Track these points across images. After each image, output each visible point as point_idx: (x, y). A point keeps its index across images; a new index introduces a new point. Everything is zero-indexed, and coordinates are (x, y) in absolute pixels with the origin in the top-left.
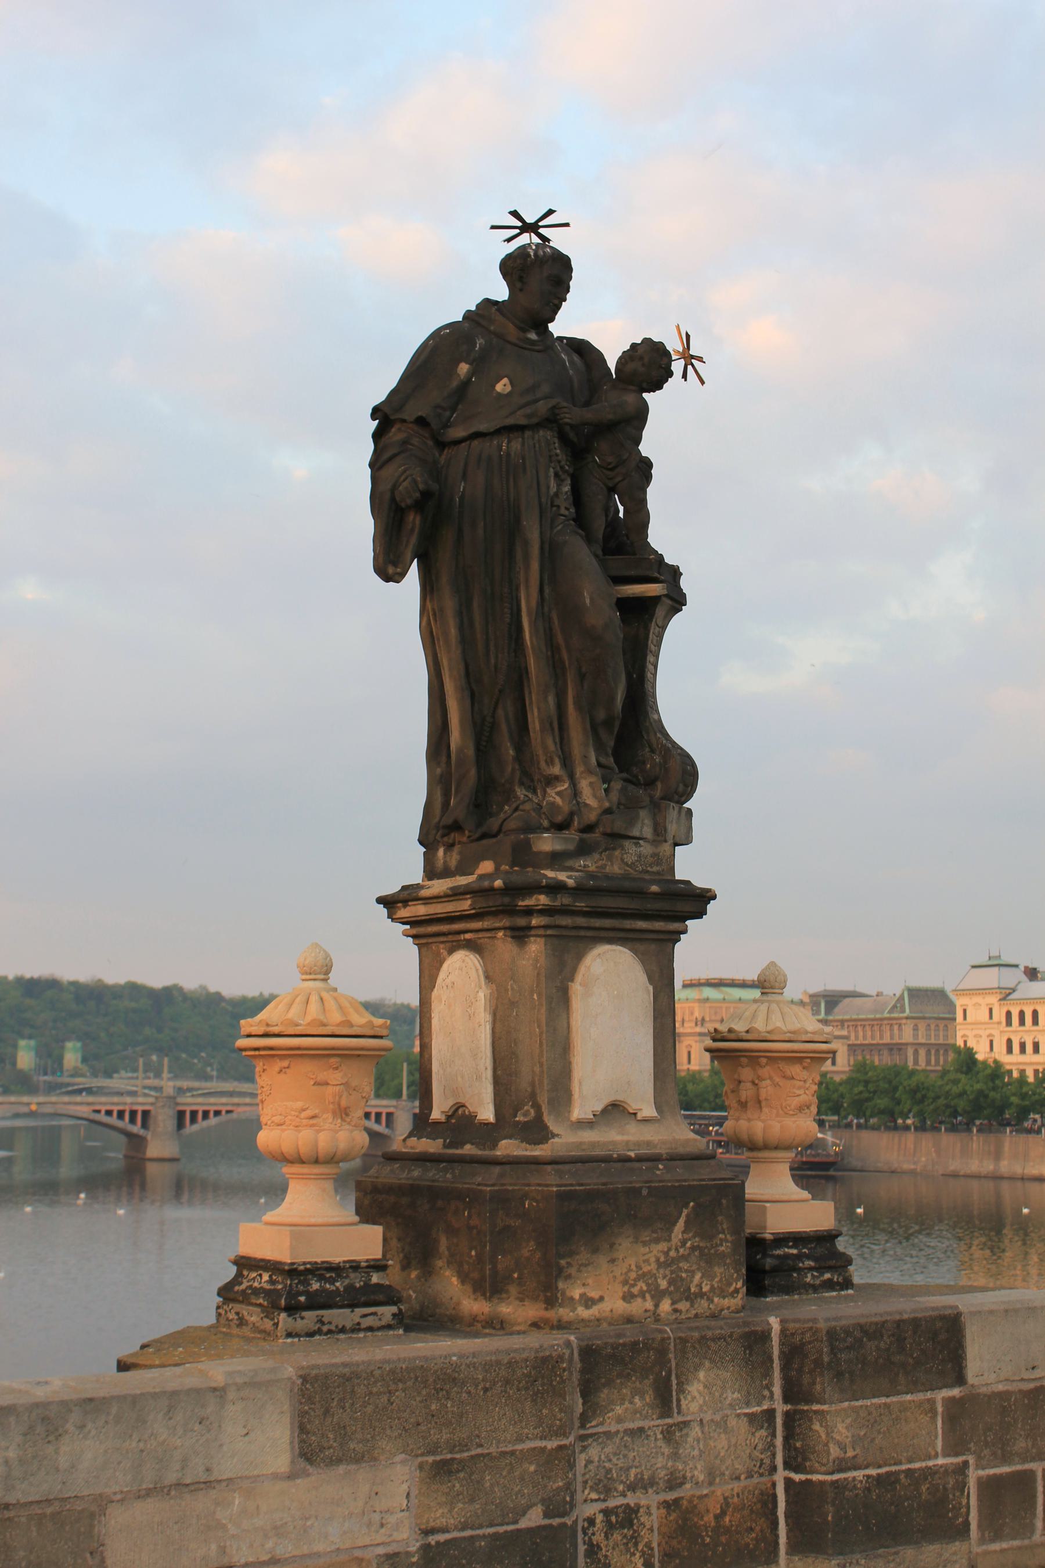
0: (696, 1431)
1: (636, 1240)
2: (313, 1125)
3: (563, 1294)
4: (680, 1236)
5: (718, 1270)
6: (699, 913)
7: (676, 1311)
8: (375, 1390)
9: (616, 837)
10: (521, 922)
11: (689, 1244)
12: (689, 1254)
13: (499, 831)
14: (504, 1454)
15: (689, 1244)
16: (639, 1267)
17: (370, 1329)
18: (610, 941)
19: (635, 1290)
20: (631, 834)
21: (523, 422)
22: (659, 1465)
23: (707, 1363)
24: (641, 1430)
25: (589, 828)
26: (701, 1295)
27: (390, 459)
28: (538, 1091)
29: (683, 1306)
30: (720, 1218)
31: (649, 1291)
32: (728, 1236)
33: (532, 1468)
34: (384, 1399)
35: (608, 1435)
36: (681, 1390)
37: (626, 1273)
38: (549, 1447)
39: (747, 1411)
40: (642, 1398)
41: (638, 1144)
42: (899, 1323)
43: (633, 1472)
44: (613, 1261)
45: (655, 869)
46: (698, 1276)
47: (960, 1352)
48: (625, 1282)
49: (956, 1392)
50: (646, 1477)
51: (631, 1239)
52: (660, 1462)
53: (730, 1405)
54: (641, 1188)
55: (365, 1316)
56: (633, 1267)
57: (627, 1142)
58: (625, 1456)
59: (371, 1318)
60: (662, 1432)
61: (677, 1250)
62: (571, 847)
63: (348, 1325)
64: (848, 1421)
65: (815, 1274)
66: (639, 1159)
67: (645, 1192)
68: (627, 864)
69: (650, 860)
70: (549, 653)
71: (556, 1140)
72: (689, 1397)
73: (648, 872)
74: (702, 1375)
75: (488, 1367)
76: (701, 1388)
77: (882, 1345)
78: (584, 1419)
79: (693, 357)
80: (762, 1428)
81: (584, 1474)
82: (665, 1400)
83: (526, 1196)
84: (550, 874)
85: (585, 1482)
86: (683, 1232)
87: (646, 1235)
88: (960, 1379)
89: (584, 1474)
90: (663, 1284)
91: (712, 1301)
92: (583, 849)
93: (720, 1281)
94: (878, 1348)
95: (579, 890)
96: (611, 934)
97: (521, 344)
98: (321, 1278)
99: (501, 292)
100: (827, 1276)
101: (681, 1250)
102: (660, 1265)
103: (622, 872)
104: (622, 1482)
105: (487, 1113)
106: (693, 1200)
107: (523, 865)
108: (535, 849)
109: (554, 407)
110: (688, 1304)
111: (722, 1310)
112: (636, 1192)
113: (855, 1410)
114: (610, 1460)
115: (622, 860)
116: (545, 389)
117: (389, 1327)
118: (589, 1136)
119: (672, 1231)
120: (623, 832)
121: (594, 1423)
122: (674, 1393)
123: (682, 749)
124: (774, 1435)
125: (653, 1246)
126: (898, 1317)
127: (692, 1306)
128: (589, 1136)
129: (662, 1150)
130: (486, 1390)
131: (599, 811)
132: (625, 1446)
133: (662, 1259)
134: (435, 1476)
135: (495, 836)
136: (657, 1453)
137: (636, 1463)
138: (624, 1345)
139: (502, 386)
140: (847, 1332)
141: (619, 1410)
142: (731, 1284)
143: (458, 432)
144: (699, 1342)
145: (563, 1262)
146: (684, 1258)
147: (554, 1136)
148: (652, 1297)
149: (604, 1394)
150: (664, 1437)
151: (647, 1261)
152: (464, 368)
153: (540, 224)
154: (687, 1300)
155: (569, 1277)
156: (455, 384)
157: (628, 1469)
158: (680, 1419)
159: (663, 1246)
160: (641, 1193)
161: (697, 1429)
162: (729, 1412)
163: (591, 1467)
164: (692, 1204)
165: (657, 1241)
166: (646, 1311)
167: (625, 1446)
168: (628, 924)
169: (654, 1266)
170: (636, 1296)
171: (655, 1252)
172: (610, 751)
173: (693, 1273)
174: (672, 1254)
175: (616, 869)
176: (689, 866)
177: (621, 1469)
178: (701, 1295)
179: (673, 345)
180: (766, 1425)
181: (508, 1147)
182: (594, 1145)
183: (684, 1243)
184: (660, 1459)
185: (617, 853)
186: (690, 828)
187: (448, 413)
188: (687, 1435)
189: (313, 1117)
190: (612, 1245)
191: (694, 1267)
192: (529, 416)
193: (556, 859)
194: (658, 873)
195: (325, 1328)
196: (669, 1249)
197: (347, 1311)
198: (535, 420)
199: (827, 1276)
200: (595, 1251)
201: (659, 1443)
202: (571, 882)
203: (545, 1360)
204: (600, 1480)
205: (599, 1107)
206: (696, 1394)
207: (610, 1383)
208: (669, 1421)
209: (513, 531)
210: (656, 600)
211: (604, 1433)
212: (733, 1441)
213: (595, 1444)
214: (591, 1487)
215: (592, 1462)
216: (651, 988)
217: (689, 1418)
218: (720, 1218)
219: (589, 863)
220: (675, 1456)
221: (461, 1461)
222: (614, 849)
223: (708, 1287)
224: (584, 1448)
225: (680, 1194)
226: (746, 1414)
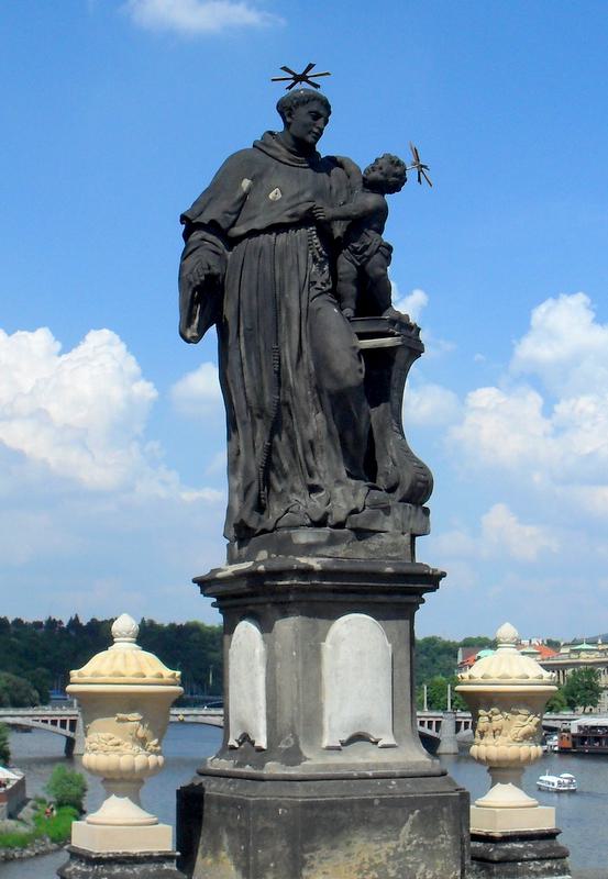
1: (369, 839)
2: (117, 751)
5: (440, 862)
6: (435, 587)
9: (362, 534)
10: (282, 598)
12: (415, 850)
13: (275, 529)
16: (371, 860)
20: (372, 528)
21: (287, 220)
25: (340, 525)
27: (191, 253)
28: (296, 726)
30: (441, 822)
41: (377, 766)
44: (349, 855)
45: (394, 555)
46: (422, 867)
56: (367, 860)
57: (367, 764)
61: (404, 847)
62: (323, 539)
66: (375, 777)
67: (376, 802)
69: (391, 548)
70: (316, 395)
71: (307, 763)
79: (422, 166)
83: (280, 805)
84: (303, 560)
87: (377, 836)
92: (332, 541)
95: (325, 574)
97: (289, 162)
99: (278, 125)
102: (389, 858)
105: (262, 742)
107: (287, 554)
108: (295, 541)
109: (311, 209)
116: (308, 195)
123: (418, 461)
125: (383, 844)
129: (397, 772)
131: (347, 512)
135: (272, 531)
139: (274, 195)
143: (239, 230)
145: (307, 856)
146: (406, 853)
147: (306, 759)
151: (379, 856)
152: (246, 183)
153: (308, 75)
155: (312, 867)
156: (239, 195)
159: (393, 844)
164: (417, 811)
168: (369, 598)
169: (384, 859)
172: (361, 465)
173: (418, 864)
175: (362, 555)
176: (428, 553)
179: (407, 159)
181: (273, 768)
182: (338, 767)
183: (410, 842)
186: (428, 522)
187: (234, 217)
189: (118, 745)
190: (348, 844)
192: (292, 216)
193: (309, 549)
196: (398, 846)
198: (295, 219)
199: (548, 864)
200: (334, 847)
202: (317, 566)
205: (345, 738)
209: (277, 303)
210: (393, 349)
216: (390, 646)
218: (441, 822)
219: (341, 550)
225: (409, 803)
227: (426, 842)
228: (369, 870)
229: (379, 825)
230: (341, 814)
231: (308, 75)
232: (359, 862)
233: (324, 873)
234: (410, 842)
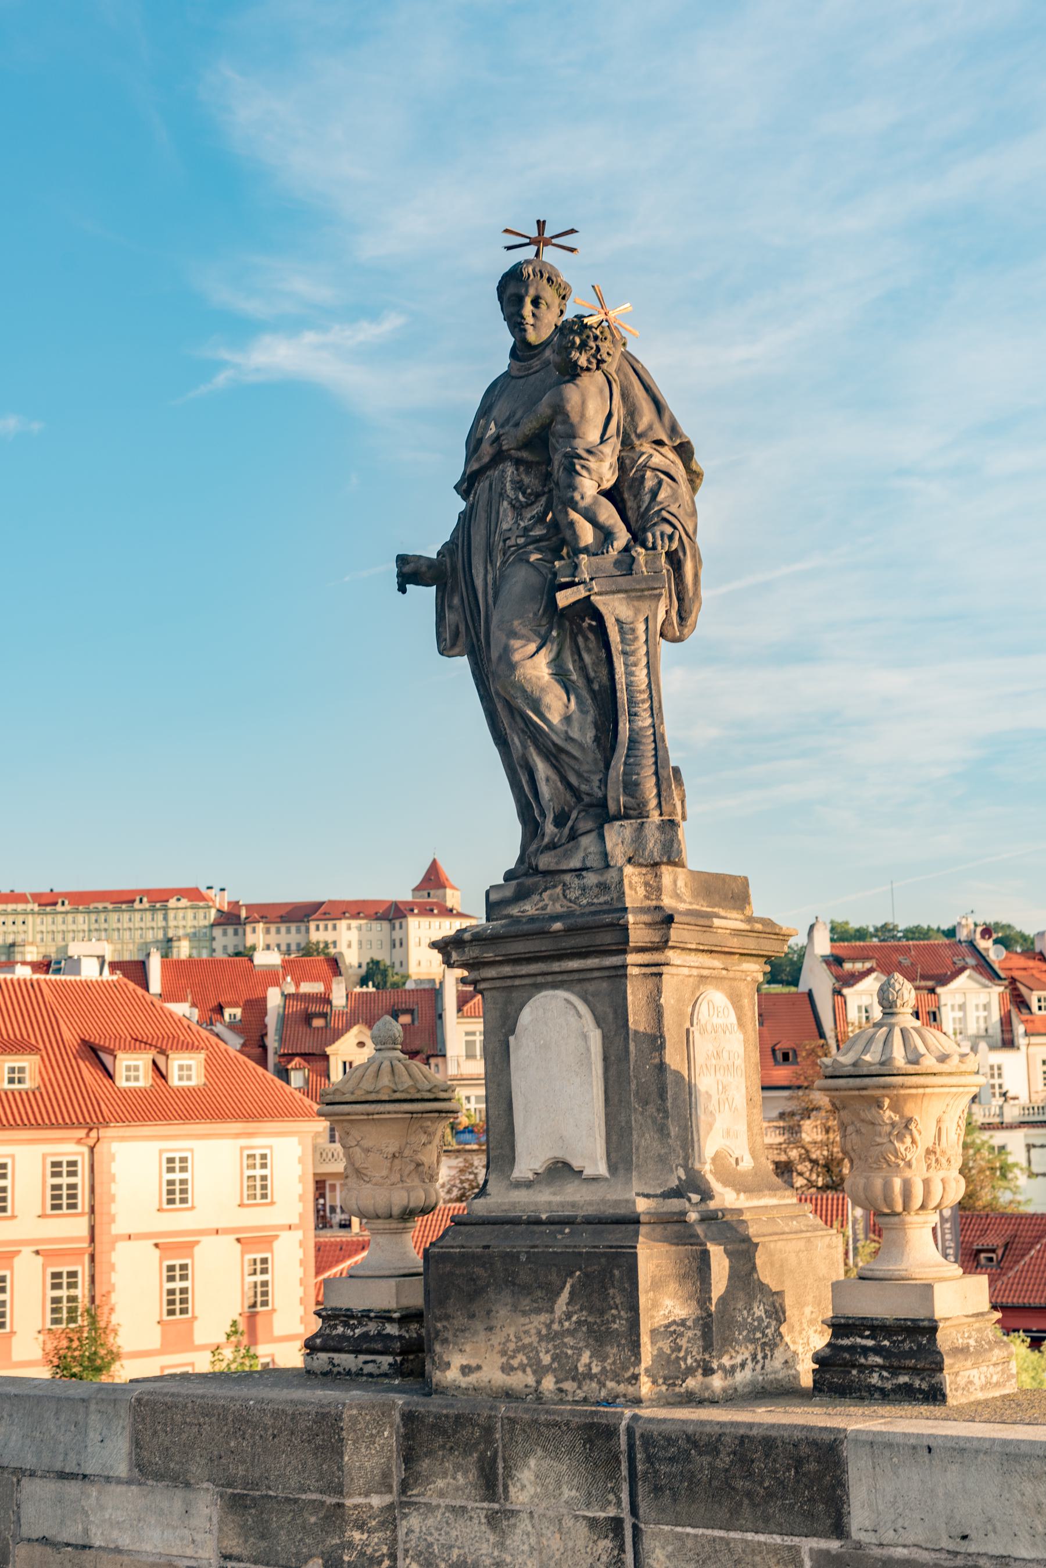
0: (524, 1524)
1: (515, 1308)
3: (441, 1358)
4: (564, 1309)
7: (561, 1390)
8: (188, 1420)
11: (574, 1318)
14: (288, 1500)
15: (574, 1318)
16: (519, 1339)
17: (370, 1375)
18: (555, 986)
19: (515, 1363)
20: (565, 868)
22: (484, 1552)
23: (540, 1452)
24: (463, 1508)
26: (589, 1376)
29: (569, 1386)
30: (611, 1291)
31: (531, 1366)
32: (622, 1313)
33: (313, 1520)
34: (195, 1429)
35: (430, 1508)
36: (509, 1475)
37: (504, 1344)
38: (328, 1502)
39: (590, 1514)
40: (465, 1473)
42: (742, 1438)
43: (455, 1552)
44: (490, 1329)
45: (602, 899)
46: (585, 1358)
47: (839, 1492)
48: (503, 1353)
49: (834, 1545)
50: (469, 1561)
51: (509, 1308)
52: (485, 1548)
53: (566, 1502)
54: (519, 1253)
55: (366, 1362)
56: (512, 1337)
58: (447, 1533)
59: (371, 1365)
60: (486, 1517)
61: (560, 1322)
63: (354, 1370)
64: (670, 1548)
65: (885, 1374)
67: (523, 1258)
68: (570, 901)
72: (518, 1484)
73: (593, 904)
74: (532, 1462)
75: (276, 1414)
76: (533, 1478)
77: (720, 1464)
78: (405, 1487)
80: (606, 1537)
81: (405, 1542)
82: (491, 1483)
85: (407, 1551)
86: (568, 1304)
87: (526, 1303)
88: (839, 1530)
89: (405, 1542)
90: (546, 1359)
91: (604, 1385)
93: (614, 1363)
94: (712, 1467)
96: (549, 978)
98: (346, 1324)
100: (903, 1379)
101: (566, 1324)
102: (541, 1338)
103: (565, 909)
104: (444, 1560)
106: (580, 1269)
110: (575, 1385)
111: (617, 1397)
112: (514, 1257)
113: (679, 1537)
114: (431, 1534)
117: (385, 1375)
118: (521, 1196)
119: (554, 1302)
120: (553, 867)
121: (414, 1492)
122: (500, 1478)
124: (622, 1549)
125: (533, 1316)
126: (742, 1432)
127: (579, 1387)
128: (521, 1196)
130: (274, 1436)
132: (447, 1523)
133: (544, 1332)
134: (232, 1507)
136: (481, 1538)
137: (458, 1543)
138: (447, 1416)
140: (670, 1441)
141: (440, 1483)
142: (628, 1368)
144: (530, 1427)
145: (439, 1325)
146: (571, 1333)
148: (534, 1372)
149: (425, 1464)
150: (489, 1522)
154: (574, 1379)
155: (445, 1341)
157: (451, 1547)
158: (509, 1507)
159: (544, 1317)
160: (518, 1258)
161: (527, 1522)
162: (564, 1511)
163: (412, 1536)
164: (578, 1273)
165: (538, 1311)
166: (526, 1386)
167: (447, 1523)
168: (556, 966)
169: (534, 1339)
170: (516, 1369)
171: (536, 1323)
173: (581, 1349)
174: (556, 1327)
177: (443, 1545)
178: (589, 1376)
180: (611, 1535)
183: (569, 1316)
184: (485, 1545)
185: (559, 890)
188: (515, 1525)
191: (582, 1344)
194: (606, 903)
195: (335, 1370)
196: (552, 1322)
197: (353, 1356)
200: (472, 1316)
201: (483, 1528)
203: (324, 1416)
204: (421, 1553)
206: (526, 1483)
207: (430, 1453)
208: (496, 1506)
211: (425, 1504)
212: (570, 1544)
213: (415, 1513)
214: (412, 1557)
215: (412, 1531)
217: (518, 1507)
218: (611, 1291)
220: (501, 1545)
221: (253, 1499)
222: (555, 886)
223: (599, 1368)
224: (405, 1516)
225: (567, 1263)
226: (585, 1517)
227: (590, 1319)
228: (517, 1351)
229: (526, 1289)
230: (479, 1271)
232: (503, 1340)
233: (461, 1350)
234: (569, 1316)
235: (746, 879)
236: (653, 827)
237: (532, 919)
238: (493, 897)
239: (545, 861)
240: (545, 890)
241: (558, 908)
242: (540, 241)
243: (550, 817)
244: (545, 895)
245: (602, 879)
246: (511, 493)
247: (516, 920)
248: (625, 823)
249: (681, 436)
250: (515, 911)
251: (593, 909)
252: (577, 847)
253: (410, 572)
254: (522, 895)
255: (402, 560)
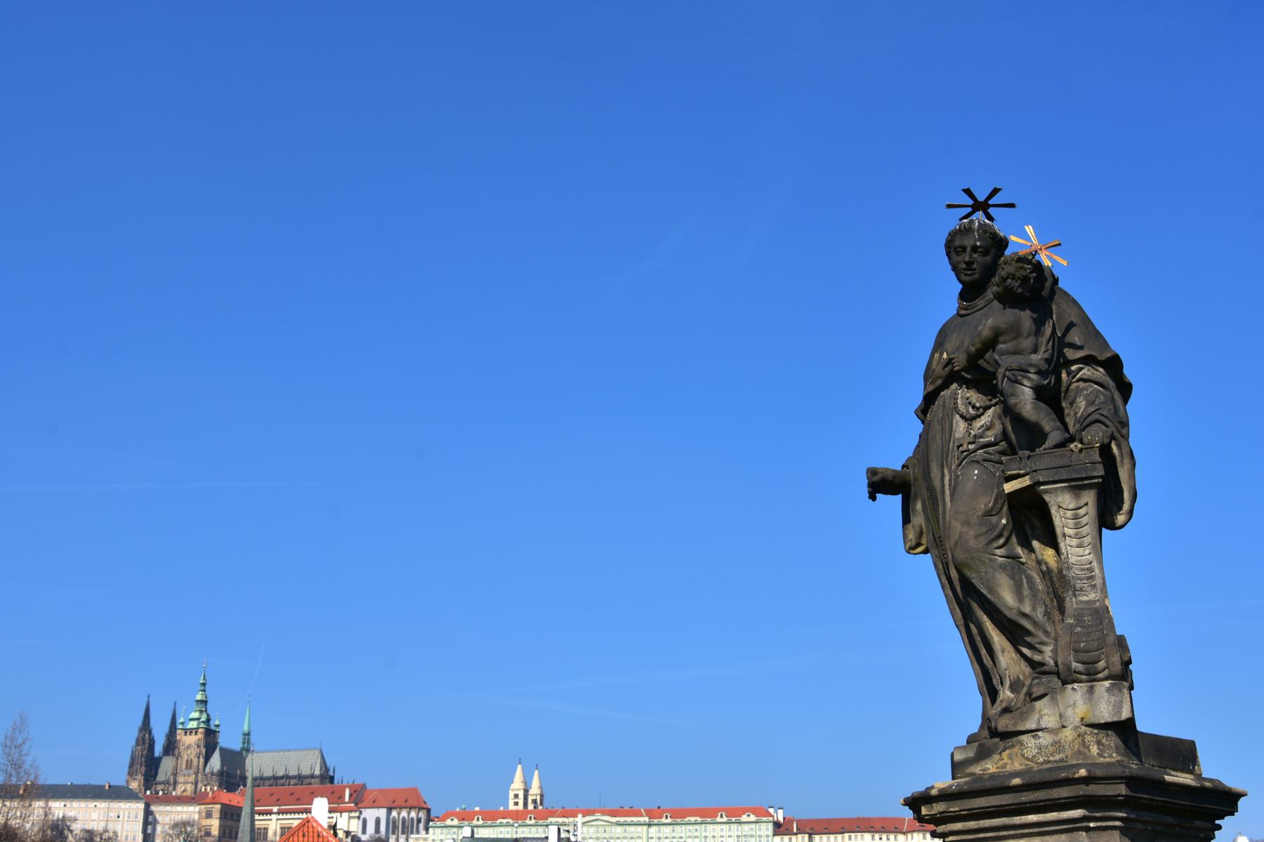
45: (1057, 757)
62: (971, 754)
68: (1028, 759)
73: (1049, 762)
115: (1023, 755)
120: (1011, 728)
168: (1017, 820)
185: (1016, 749)
194: (1061, 760)
222: (1013, 746)
231: (991, 202)
235: (1193, 743)
236: (1103, 689)
237: (993, 776)
238: (958, 757)
239: (1004, 724)
240: (1004, 750)
241: (1017, 766)
242: (981, 206)
243: (1007, 683)
244: (1005, 755)
245: (1056, 738)
246: (962, 408)
247: (979, 778)
248: (1075, 686)
249: (1111, 350)
250: (977, 769)
251: (1049, 765)
252: (1032, 710)
253: (880, 484)
254: (983, 754)
255: (872, 472)
